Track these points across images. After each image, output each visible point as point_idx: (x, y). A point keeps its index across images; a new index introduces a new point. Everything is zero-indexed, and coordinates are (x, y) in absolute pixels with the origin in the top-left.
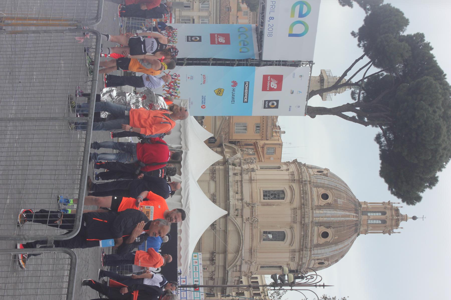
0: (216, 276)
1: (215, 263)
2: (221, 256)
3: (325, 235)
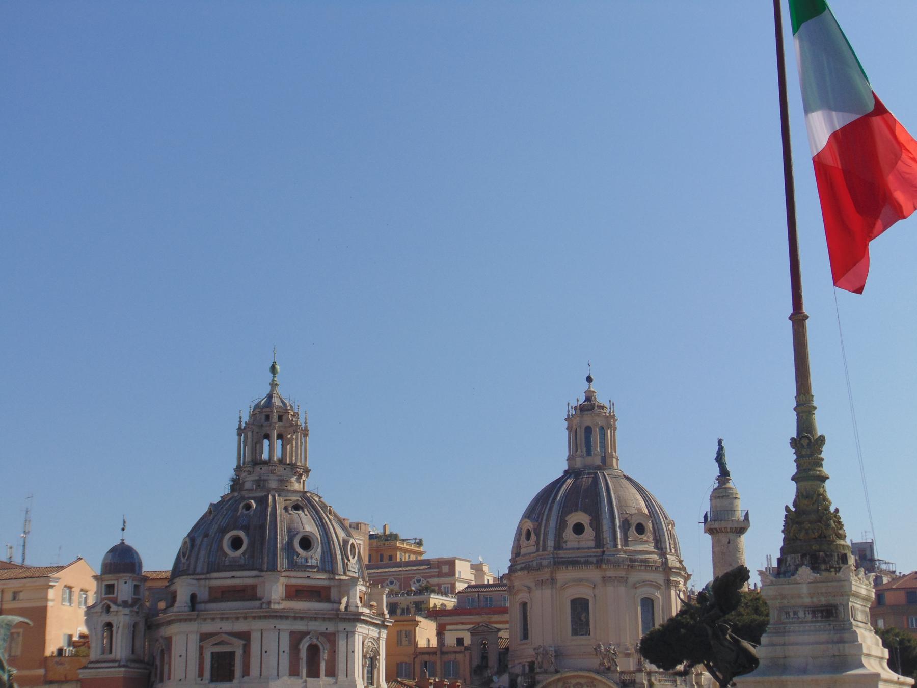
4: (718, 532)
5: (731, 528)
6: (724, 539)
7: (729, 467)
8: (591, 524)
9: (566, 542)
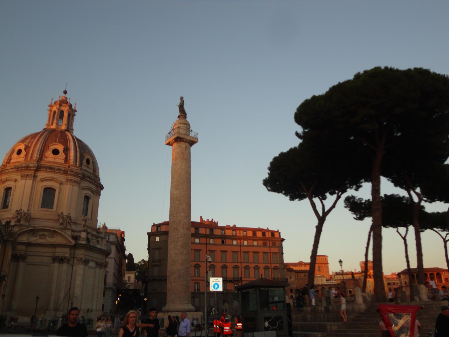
0: (82, 256)
1: (65, 257)
2: (58, 250)
3: (56, 152)
4: (181, 141)
5: (189, 140)
6: (183, 145)
7: (187, 111)
8: (64, 151)
9: (47, 157)
